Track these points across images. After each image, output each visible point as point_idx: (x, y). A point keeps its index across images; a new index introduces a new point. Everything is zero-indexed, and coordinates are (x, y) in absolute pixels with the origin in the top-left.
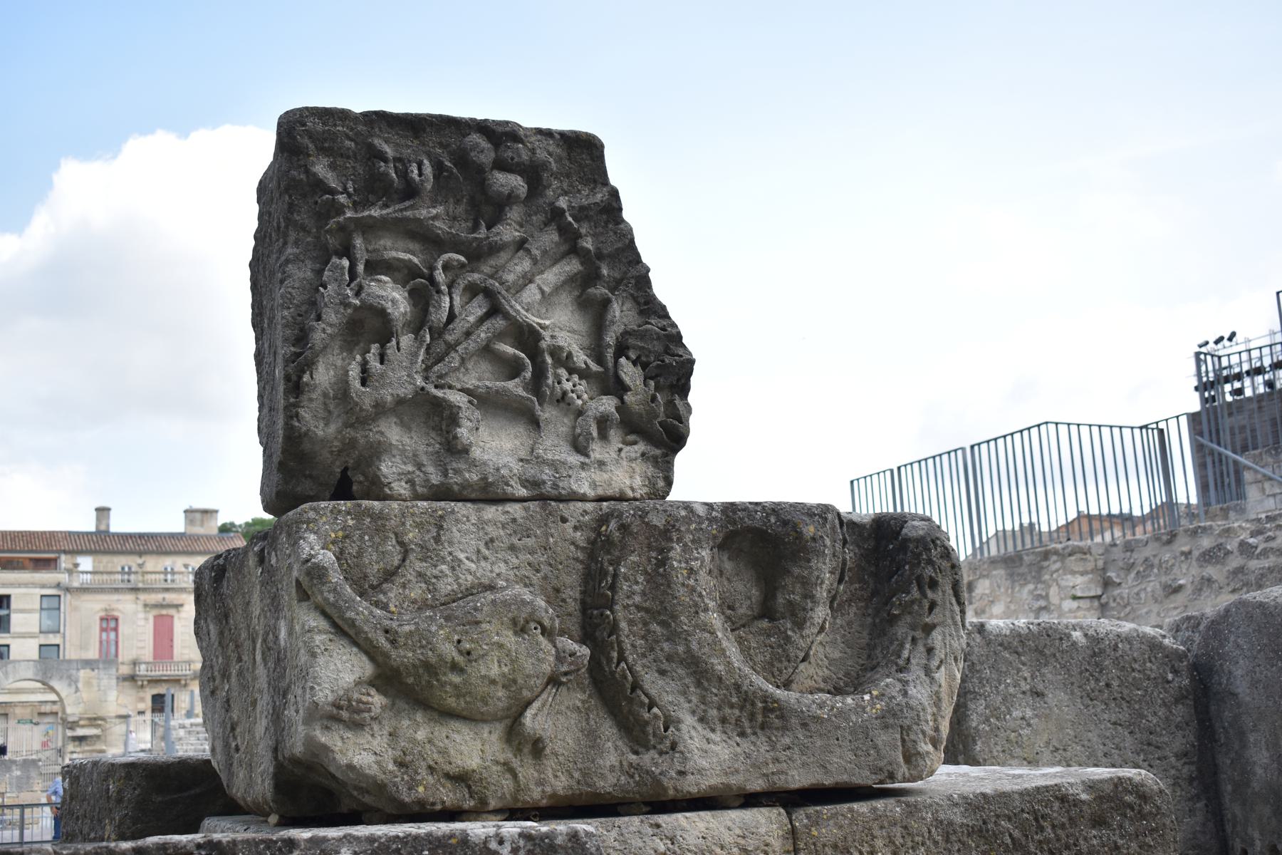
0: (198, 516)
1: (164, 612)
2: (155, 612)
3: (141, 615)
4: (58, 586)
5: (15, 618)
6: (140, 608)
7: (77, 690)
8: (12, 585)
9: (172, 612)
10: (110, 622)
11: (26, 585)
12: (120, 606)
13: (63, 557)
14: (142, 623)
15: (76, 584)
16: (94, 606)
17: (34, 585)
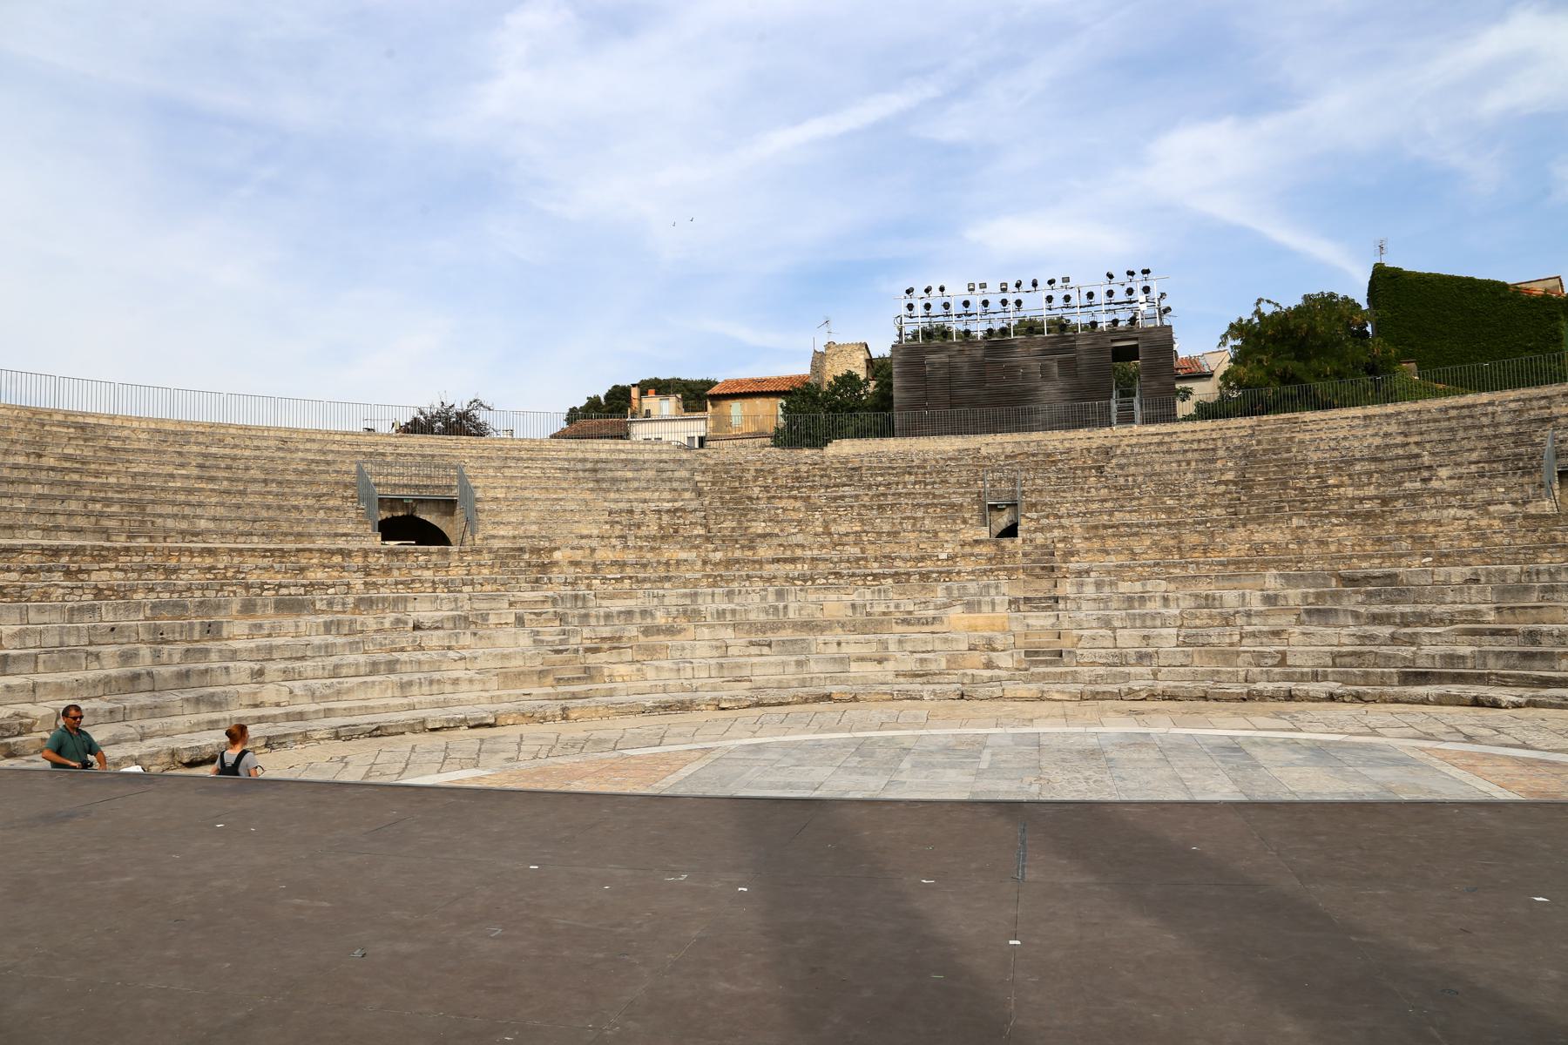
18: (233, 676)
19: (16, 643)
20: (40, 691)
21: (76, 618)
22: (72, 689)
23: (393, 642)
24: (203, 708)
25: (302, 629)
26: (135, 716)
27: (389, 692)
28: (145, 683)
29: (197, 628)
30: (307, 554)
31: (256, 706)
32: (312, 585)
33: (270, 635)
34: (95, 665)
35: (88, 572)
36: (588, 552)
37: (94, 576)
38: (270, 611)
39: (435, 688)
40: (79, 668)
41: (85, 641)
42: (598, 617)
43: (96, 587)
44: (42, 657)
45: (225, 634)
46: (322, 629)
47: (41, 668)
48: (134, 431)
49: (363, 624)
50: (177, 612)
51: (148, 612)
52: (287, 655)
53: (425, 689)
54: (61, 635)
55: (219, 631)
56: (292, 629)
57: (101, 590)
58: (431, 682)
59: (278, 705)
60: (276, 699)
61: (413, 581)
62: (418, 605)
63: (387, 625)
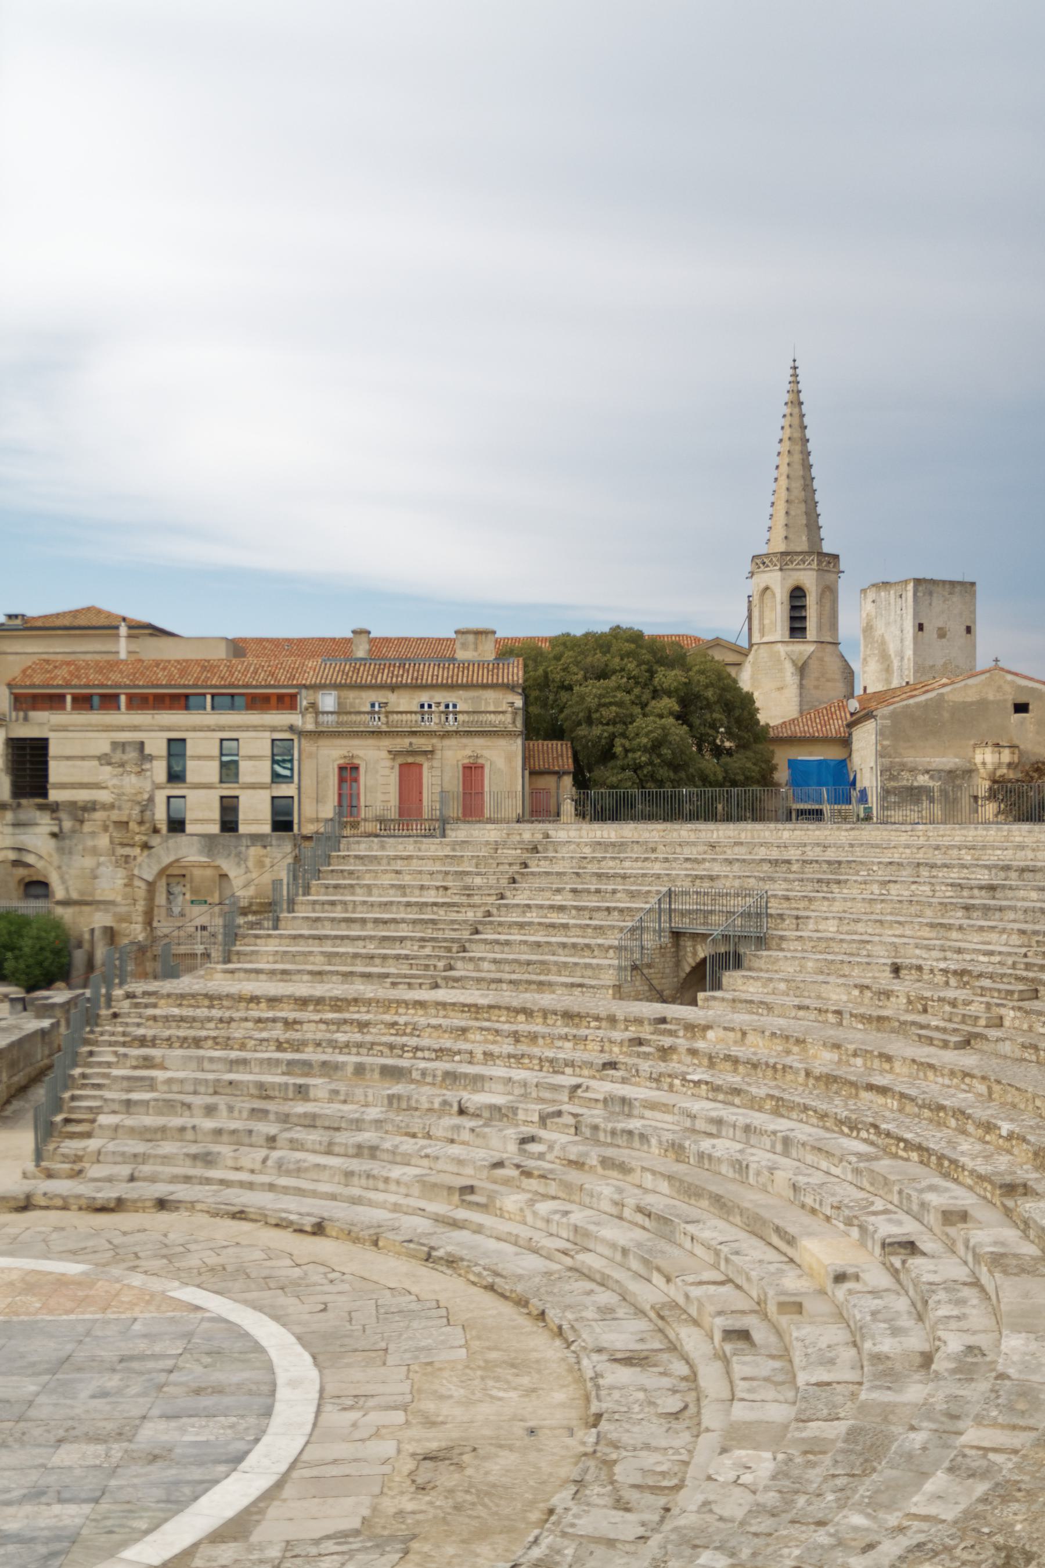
0: (471, 638)
1: (410, 760)
2: (400, 760)
3: (389, 763)
4: (291, 728)
5: (243, 765)
6: (384, 754)
7: (248, 871)
8: (239, 728)
9: (419, 759)
10: (348, 772)
11: (255, 728)
12: (360, 753)
13: (304, 692)
14: (387, 772)
15: (310, 726)
16: (331, 754)
17: (262, 728)
18: (254, 1139)
19: (165, 1088)
20: (120, 1131)
21: (234, 1068)
22: (140, 1133)
23: (408, 1126)
24: (199, 1164)
25: (370, 1099)
26: (151, 1161)
27: (336, 1179)
28: (189, 1135)
29: (291, 1088)
30: (497, 1012)
31: (237, 1169)
32: (441, 1050)
33: (345, 1102)
34: (187, 1113)
35: (301, 1023)
36: (739, 1035)
37: (305, 1027)
38: (376, 1076)
39: (371, 1182)
40: (176, 1114)
41: (211, 1090)
42: (605, 1131)
43: (277, 1040)
44: (152, 1103)
45: (312, 1095)
46: (386, 1101)
47: (151, 1111)
48: (578, 844)
49: (417, 1101)
50: (306, 1069)
51: (284, 1068)
52: (327, 1124)
53: (363, 1182)
54: (195, 1084)
55: (307, 1093)
56: (362, 1098)
57: (281, 1043)
58: (368, 1176)
59: (252, 1171)
60: (250, 1166)
61: (523, 1056)
62: (493, 1086)
63: (436, 1106)
